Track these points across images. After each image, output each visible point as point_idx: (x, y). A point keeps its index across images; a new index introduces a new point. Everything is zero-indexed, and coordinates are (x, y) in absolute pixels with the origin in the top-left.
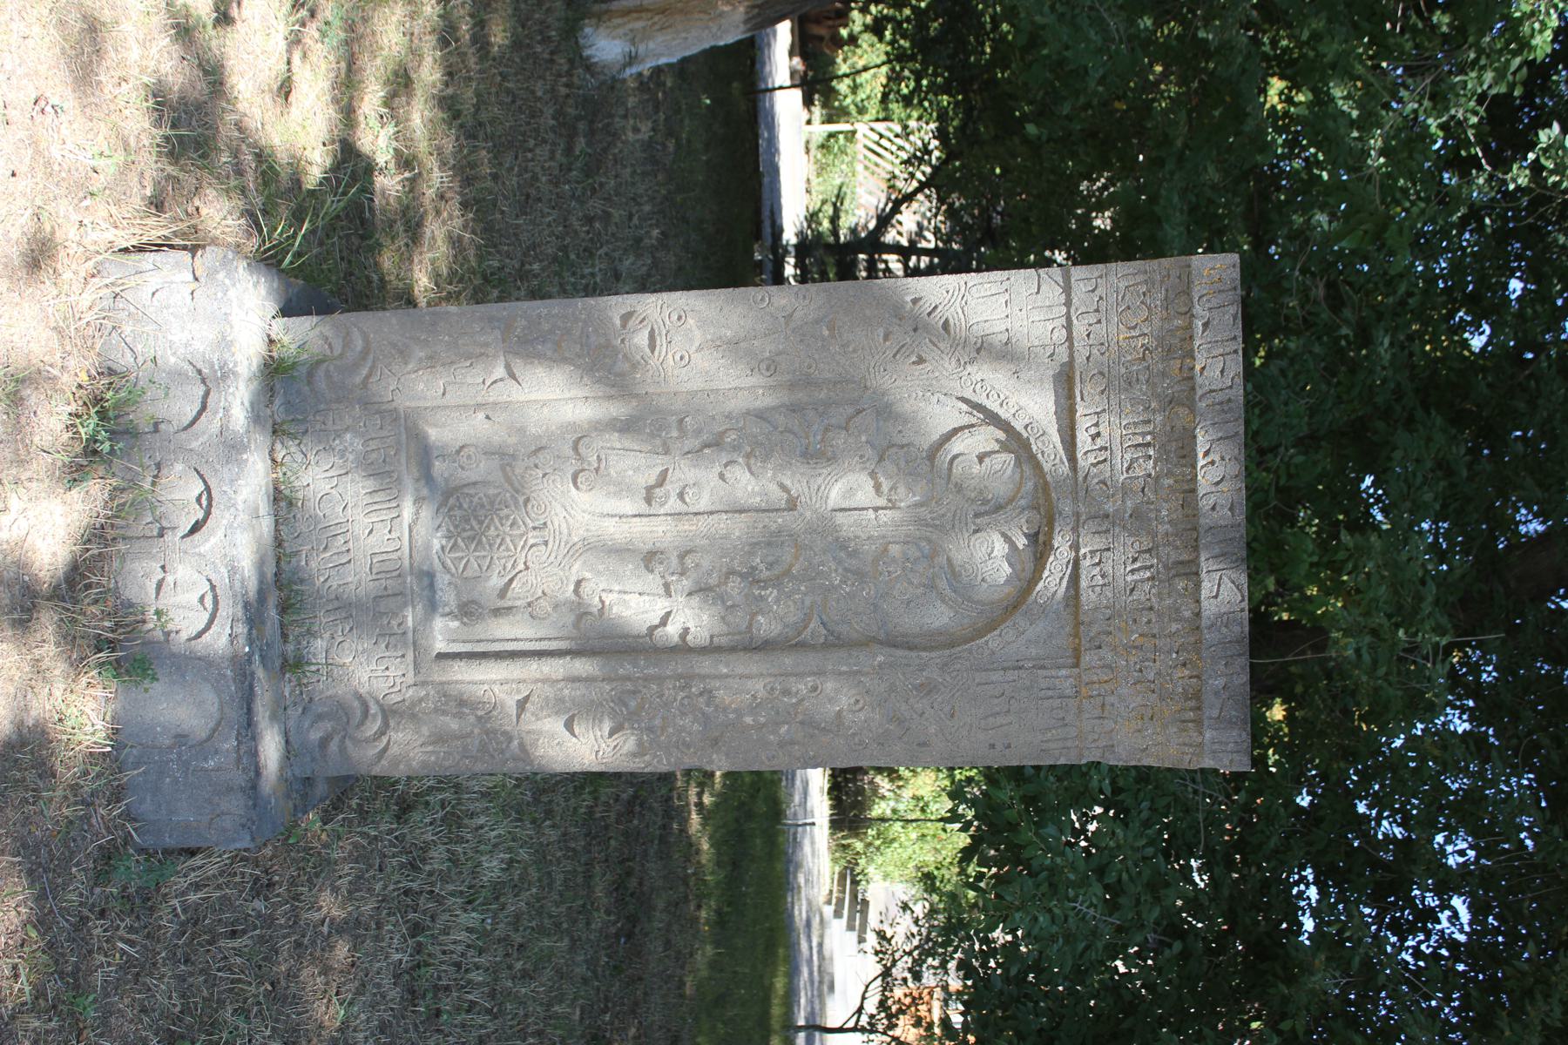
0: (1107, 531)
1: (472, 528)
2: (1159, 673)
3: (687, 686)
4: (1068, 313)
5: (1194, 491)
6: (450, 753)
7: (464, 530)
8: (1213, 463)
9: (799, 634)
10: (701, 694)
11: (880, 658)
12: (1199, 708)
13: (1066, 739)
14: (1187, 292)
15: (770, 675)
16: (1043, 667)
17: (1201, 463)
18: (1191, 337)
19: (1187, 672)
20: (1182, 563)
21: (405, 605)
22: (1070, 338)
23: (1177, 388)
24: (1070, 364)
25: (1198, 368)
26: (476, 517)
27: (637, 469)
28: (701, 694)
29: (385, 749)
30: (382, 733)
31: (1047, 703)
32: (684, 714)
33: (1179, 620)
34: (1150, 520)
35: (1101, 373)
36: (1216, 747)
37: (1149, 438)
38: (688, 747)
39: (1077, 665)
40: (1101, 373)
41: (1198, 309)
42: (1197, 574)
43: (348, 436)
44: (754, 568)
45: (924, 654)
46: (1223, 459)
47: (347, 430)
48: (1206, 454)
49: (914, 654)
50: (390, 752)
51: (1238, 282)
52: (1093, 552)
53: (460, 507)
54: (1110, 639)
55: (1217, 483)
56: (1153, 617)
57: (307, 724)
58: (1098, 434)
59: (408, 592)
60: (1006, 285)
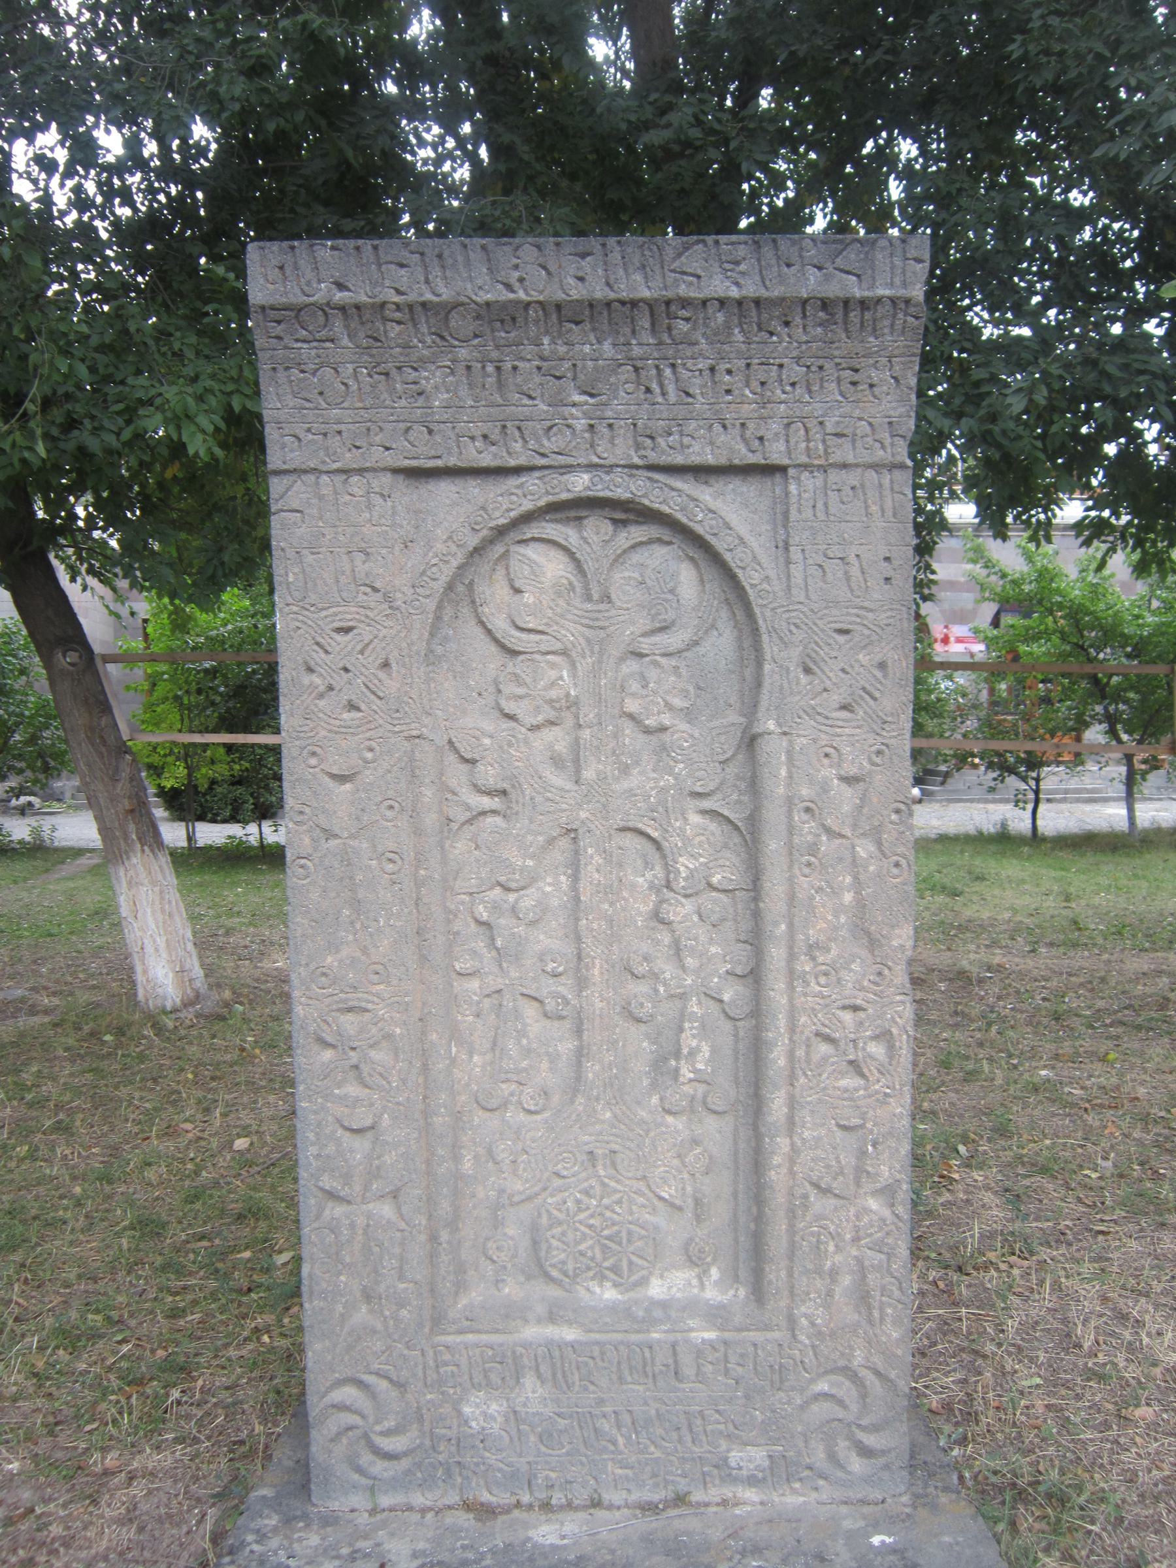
0: (610, 426)
1: (591, 1248)
2: (798, 360)
3: (803, 976)
5: (559, 307)
6: (883, 1289)
7: (592, 1259)
8: (521, 280)
9: (737, 828)
10: (813, 959)
11: (771, 725)
12: (846, 302)
13: (881, 485)
14: (298, 310)
15: (791, 867)
16: (786, 514)
17: (522, 295)
18: (358, 307)
19: (798, 320)
20: (653, 324)
21: (687, 1341)
22: (361, 471)
23: (424, 328)
24: (396, 471)
25: (397, 299)
26: (577, 1243)
27: (522, 1033)
28: (813, 959)
29: (877, 1373)
30: (854, 1378)
31: (832, 510)
32: (839, 981)
33: (728, 327)
34: (596, 368)
35: (408, 430)
36: (897, 281)
37: (490, 369)
38: (880, 974)
39: (782, 469)
40: (408, 430)
42: (668, 303)
43: (467, 1410)
45: (767, 668)
46: (516, 267)
47: (459, 1413)
48: (509, 287)
49: (767, 682)
50: (880, 1367)
51: (285, 244)
52: (638, 447)
53: (564, 1263)
54: (751, 425)
55: (549, 273)
57: (840, 1474)
58: (485, 437)
59: (671, 1337)
60: (290, 553)
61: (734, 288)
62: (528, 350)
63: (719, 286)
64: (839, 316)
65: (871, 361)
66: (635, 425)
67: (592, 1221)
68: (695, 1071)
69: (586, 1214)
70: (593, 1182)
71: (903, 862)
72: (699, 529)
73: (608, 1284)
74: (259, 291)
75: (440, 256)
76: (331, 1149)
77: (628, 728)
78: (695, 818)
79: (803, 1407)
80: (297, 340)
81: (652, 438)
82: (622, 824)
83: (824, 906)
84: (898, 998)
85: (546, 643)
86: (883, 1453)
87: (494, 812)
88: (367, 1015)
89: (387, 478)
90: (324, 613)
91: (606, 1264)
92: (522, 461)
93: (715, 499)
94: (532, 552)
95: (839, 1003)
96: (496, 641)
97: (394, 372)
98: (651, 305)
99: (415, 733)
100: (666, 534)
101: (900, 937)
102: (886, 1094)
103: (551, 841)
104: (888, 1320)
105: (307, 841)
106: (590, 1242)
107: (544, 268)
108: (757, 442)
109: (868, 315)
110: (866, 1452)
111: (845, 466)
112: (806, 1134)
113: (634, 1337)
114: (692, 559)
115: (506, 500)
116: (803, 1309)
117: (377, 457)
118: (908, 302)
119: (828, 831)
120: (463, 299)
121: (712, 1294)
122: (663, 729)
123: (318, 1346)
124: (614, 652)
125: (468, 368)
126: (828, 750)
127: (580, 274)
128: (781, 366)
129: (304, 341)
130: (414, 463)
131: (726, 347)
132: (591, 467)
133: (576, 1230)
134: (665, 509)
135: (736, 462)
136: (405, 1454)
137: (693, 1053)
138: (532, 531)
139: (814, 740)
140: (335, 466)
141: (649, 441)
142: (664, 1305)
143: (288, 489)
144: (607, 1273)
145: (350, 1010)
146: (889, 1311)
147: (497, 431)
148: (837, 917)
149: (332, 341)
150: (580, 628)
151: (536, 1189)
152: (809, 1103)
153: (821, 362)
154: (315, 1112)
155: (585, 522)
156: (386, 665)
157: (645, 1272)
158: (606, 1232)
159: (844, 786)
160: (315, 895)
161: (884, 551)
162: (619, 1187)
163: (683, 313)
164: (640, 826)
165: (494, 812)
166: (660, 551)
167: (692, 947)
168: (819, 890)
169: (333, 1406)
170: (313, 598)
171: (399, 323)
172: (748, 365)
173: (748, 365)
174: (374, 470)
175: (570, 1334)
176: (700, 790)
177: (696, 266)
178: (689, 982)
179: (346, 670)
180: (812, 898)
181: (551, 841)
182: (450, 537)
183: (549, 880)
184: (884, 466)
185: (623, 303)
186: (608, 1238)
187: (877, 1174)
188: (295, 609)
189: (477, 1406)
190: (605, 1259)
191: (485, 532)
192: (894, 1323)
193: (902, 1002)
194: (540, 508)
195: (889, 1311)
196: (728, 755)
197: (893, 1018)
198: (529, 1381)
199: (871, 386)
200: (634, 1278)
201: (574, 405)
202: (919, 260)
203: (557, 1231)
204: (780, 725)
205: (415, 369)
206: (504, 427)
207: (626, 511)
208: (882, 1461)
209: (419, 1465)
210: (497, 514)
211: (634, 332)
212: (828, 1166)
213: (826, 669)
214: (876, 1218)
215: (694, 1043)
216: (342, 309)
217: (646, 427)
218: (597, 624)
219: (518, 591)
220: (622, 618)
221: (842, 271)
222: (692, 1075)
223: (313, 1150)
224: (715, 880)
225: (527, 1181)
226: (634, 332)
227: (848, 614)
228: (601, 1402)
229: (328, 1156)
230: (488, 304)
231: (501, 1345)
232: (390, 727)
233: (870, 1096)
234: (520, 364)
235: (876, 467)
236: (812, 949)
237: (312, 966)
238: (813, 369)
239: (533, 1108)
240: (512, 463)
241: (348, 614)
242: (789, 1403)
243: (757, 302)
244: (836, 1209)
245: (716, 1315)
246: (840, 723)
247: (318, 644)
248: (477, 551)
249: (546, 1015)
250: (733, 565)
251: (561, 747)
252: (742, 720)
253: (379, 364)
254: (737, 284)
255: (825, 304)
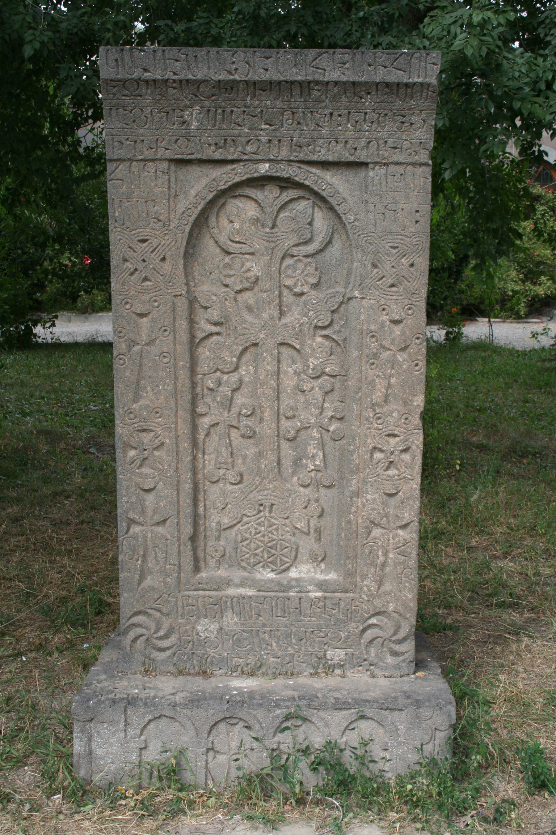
2: (374, 110)
4: (137, 161)
5: (255, 83)
7: (262, 557)
9: (339, 344)
10: (374, 410)
12: (398, 84)
14: (125, 81)
16: (366, 186)
17: (237, 77)
18: (154, 81)
20: (301, 92)
22: (153, 160)
24: (170, 161)
28: (374, 410)
37: (219, 111)
39: (366, 164)
41: (135, 76)
42: (309, 83)
43: (199, 628)
44: (295, 372)
45: (355, 264)
48: (230, 73)
50: (402, 611)
53: (247, 559)
54: (350, 142)
55: (250, 66)
56: (336, 113)
58: (216, 144)
59: (300, 595)
61: (342, 76)
62: (239, 103)
63: (333, 75)
64: (395, 91)
65: (412, 112)
66: (292, 140)
67: (262, 539)
68: (315, 465)
69: (259, 535)
70: (262, 519)
71: (420, 363)
72: (324, 194)
73: (269, 570)
74: (106, 71)
75: (196, 57)
76: (134, 499)
77: (285, 292)
78: (319, 339)
79: (364, 631)
80: (123, 95)
81: (300, 146)
82: (281, 341)
83: (380, 384)
84: (416, 431)
85: (245, 248)
86: (403, 654)
87: (218, 334)
88: (153, 434)
89: (166, 164)
90: (133, 232)
91: (269, 560)
92: (235, 157)
93: (332, 178)
94: (239, 203)
95: (387, 433)
96: (220, 247)
97: (171, 112)
98: (300, 83)
99: (179, 293)
100: (307, 195)
101: (417, 401)
102: (409, 479)
103: (245, 350)
104: (407, 589)
105: (124, 346)
106: (261, 549)
107: (248, 63)
108: (353, 151)
109: (409, 90)
110: (395, 654)
111: (397, 163)
112: (369, 497)
113: (281, 594)
114: (320, 207)
115: (225, 176)
116: (365, 583)
117: (161, 153)
118: (429, 85)
119: (383, 347)
120: (206, 78)
121: (321, 577)
122: (303, 294)
123: (126, 595)
124: (280, 255)
125: (209, 111)
126: (384, 307)
127: (266, 67)
128: (366, 113)
129: (127, 96)
130: (180, 157)
131: (339, 104)
132: (269, 161)
133: (255, 543)
134: (307, 183)
135: (343, 160)
136: (168, 649)
137: (314, 456)
138: (239, 192)
139: (378, 302)
140: (141, 157)
141: (298, 149)
142: (296, 580)
143: (116, 169)
144: (269, 564)
145: (143, 431)
146: (407, 585)
147: (222, 141)
148: (387, 390)
149: (141, 96)
150: (261, 241)
151: (235, 522)
152: (370, 482)
153: (386, 112)
154: (126, 480)
155: (266, 187)
156: (164, 259)
157: (288, 565)
158: (269, 544)
159: (392, 325)
160: (128, 374)
161: (415, 206)
162: (276, 522)
163: (317, 87)
164: (290, 342)
165: (218, 334)
166: (304, 203)
167: (315, 404)
168: (378, 376)
169: (134, 625)
170: (127, 224)
171: (175, 88)
172: (349, 113)
173: (349, 113)
174: (160, 160)
175: (250, 592)
176: (321, 325)
177: (323, 65)
178: (313, 421)
179: (144, 261)
180: (374, 380)
181: (245, 350)
182: (197, 195)
183: (244, 368)
184: (417, 164)
185: (287, 82)
186: (270, 547)
187: (403, 518)
188: (119, 229)
189: (204, 626)
190: (269, 558)
191: (214, 193)
192: (409, 591)
193: (418, 433)
194: (244, 181)
195: (407, 585)
196: (335, 308)
197: (413, 441)
198: (229, 614)
199: (412, 124)
200: (283, 567)
201: (261, 130)
202: (434, 64)
203: (245, 543)
204: (362, 293)
205: (182, 111)
206: (226, 140)
207: (287, 182)
208: (401, 658)
209: (174, 654)
210: (222, 183)
211: (292, 95)
212: (379, 513)
213: (385, 266)
214: (401, 539)
215: (315, 451)
216: (147, 82)
217: (297, 141)
218: (271, 239)
219: (231, 222)
220: (284, 237)
221: (396, 69)
222: (313, 468)
223: (125, 499)
224: (327, 370)
225: (230, 518)
226: (292, 95)
227: (397, 239)
228: (264, 625)
229: (132, 502)
230: (219, 81)
231: (216, 596)
232: (166, 290)
233: (400, 479)
234: (235, 110)
235: (413, 164)
236: (373, 406)
237: (126, 408)
238: (382, 115)
239: (234, 482)
240: (230, 158)
241: (146, 233)
242: (357, 628)
243: (354, 83)
244: (383, 535)
245: (322, 586)
246: (391, 294)
247: (130, 247)
248: (211, 203)
249: (243, 436)
250: (339, 212)
251: (251, 302)
252: (343, 290)
253: (164, 108)
254: (344, 74)
255: (388, 85)
